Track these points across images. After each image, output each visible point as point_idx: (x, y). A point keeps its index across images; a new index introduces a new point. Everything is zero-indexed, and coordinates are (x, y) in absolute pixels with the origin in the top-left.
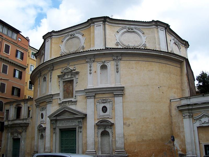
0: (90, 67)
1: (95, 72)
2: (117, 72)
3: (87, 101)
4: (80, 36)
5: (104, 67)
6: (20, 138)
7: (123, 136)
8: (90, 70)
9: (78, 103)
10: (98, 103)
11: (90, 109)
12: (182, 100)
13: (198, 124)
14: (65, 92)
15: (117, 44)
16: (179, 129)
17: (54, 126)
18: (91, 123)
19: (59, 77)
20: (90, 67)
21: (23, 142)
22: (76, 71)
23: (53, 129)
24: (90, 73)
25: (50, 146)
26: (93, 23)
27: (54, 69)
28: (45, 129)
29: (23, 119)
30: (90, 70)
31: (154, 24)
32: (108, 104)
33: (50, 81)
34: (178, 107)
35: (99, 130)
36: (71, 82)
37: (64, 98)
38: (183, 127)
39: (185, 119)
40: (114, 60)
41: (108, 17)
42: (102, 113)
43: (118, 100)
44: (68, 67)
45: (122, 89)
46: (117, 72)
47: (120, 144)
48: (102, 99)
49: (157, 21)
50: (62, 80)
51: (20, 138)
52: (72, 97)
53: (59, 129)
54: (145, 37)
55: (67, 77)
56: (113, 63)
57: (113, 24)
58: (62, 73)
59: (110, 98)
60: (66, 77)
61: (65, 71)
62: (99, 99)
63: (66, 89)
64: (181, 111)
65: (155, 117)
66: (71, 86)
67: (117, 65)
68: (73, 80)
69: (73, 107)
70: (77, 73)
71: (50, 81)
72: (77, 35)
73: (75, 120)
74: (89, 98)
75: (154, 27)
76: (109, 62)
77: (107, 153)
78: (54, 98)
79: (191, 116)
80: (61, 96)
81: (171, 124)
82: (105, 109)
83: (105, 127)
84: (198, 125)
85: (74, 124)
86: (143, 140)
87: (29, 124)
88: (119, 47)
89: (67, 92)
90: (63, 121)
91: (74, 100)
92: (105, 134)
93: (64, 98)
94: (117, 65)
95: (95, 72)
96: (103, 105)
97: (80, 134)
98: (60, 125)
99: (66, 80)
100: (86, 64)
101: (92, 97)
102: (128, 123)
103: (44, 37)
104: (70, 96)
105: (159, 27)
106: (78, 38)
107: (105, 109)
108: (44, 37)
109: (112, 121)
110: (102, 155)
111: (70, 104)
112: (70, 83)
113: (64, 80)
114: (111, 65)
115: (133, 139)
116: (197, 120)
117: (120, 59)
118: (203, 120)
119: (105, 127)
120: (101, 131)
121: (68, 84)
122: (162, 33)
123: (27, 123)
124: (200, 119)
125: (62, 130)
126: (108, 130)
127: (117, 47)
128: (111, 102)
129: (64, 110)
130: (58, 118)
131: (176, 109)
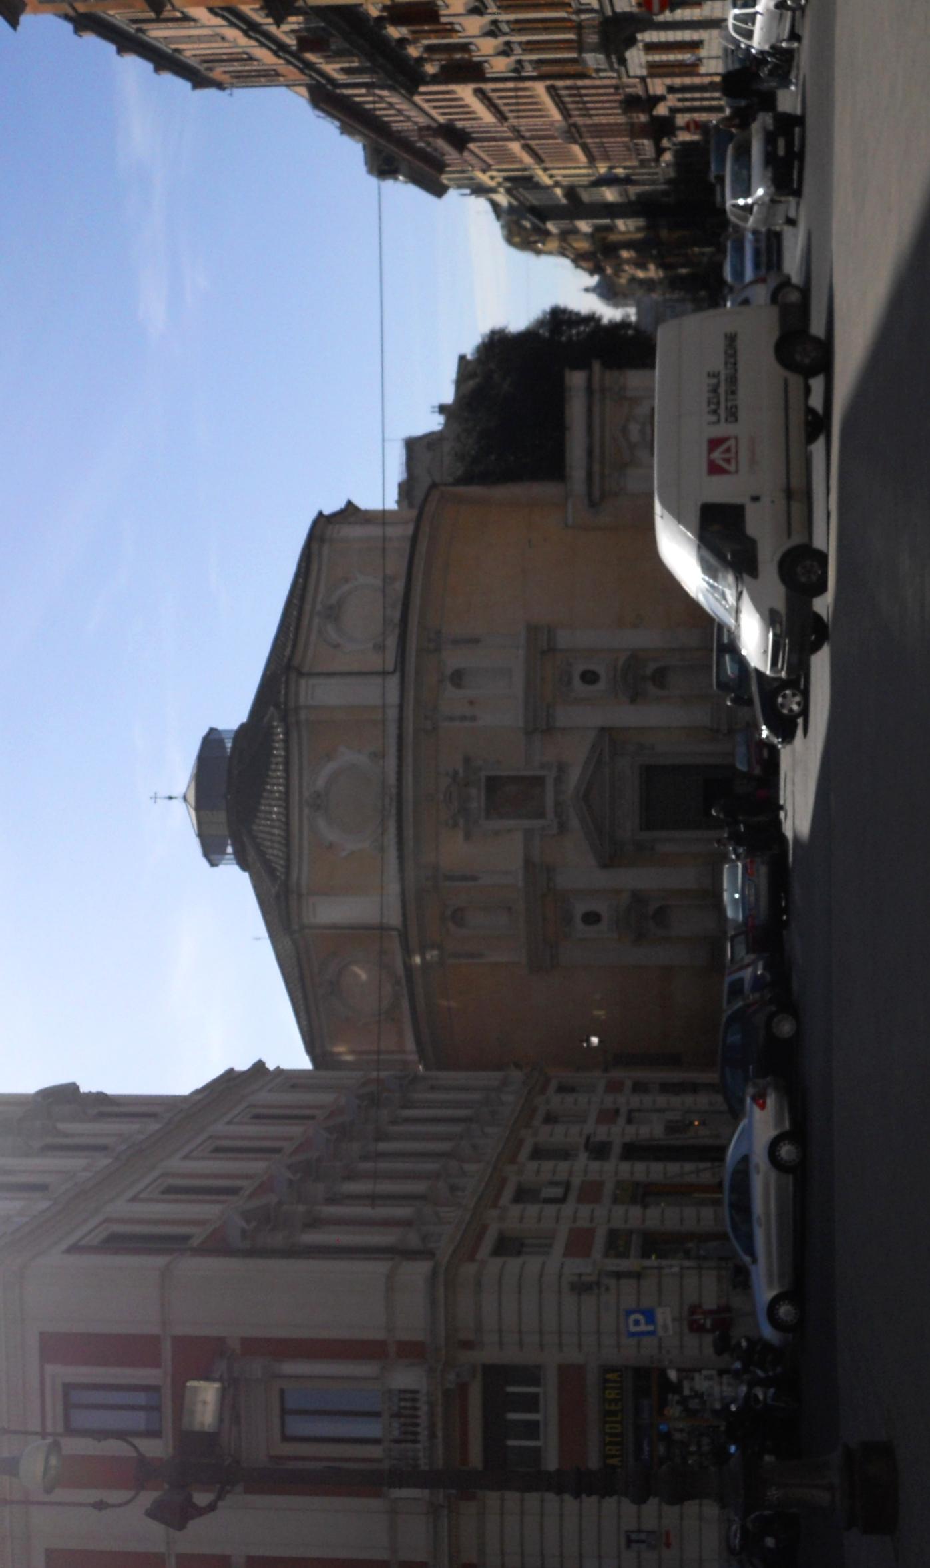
0: (451, 719)
1: (471, 703)
4: (329, 768)
5: (458, 678)
8: (463, 718)
11: (587, 716)
18: (627, 716)
20: (451, 719)
26: (297, 709)
28: (638, 899)
30: (463, 718)
33: (474, 878)
34: (592, 505)
36: (493, 784)
42: (602, 685)
43: (563, 639)
45: (533, 630)
53: (641, 829)
55: (477, 798)
58: (455, 825)
67: (456, 642)
69: (574, 776)
70: (467, 760)
71: (474, 878)
72: (320, 783)
75: (326, 550)
80: (537, 823)
82: (590, 677)
88: (392, 642)
93: (541, 815)
94: (456, 642)
95: (471, 703)
96: (577, 682)
107: (590, 677)
114: (454, 659)
117: (439, 632)
126: (651, 667)
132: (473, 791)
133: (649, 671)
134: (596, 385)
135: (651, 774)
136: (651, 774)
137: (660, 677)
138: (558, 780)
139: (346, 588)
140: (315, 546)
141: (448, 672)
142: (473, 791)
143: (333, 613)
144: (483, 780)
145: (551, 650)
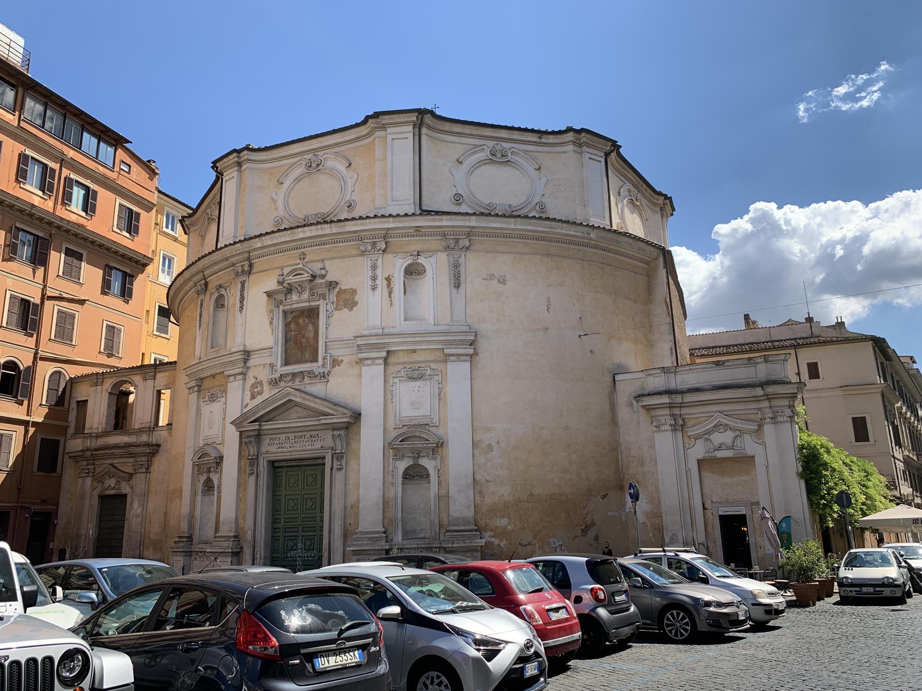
0: (374, 267)
2: (457, 286)
3: (363, 374)
6: (126, 495)
7: (471, 481)
8: (374, 278)
9: (330, 378)
10: (396, 380)
12: (650, 375)
13: (698, 451)
14: (291, 344)
15: (458, 199)
16: (642, 463)
17: (252, 454)
18: (371, 441)
19: (269, 294)
20: (374, 267)
21: (136, 505)
22: (329, 278)
23: (249, 463)
24: (374, 288)
25: (237, 518)
26: (383, 127)
27: (255, 270)
28: (219, 460)
29: (141, 431)
30: (374, 278)
31: (571, 139)
32: (428, 383)
33: (241, 308)
34: (639, 397)
35: (398, 463)
36: (312, 314)
37: (286, 363)
38: (654, 461)
39: (662, 434)
40: (447, 248)
41: (432, 113)
44: (301, 266)
46: (457, 286)
47: (461, 506)
48: (408, 367)
49: (583, 130)
50: (281, 307)
51: (126, 495)
52: (315, 359)
53: (269, 462)
54: (544, 180)
55: (298, 301)
56: (443, 257)
57: (443, 136)
58: (280, 283)
59: (433, 366)
60: (295, 297)
61: (291, 277)
62: (399, 367)
63: (293, 333)
64: (648, 409)
65: (567, 427)
66: (310, 327)
67: (456, 266)
68: (318, 308)
69: (317, 388)
72: (330, 163)
73: (320, 433)
74: (369, 362)
75: (571, 147)
76: (430, 254)
77: (422, 535)
78: (251, 363)
79: (680, 425)
81: (614, 447)
83: (415, 449)
84: (701, 456)
85: (318, 445)
86: (531, 494)
87: (159, 446)
89: (296, 344)
90: (283, 437)
91: (321, 370)
92: (415, 474)
94: (456, 266)
97: (339, 476)
98: (273, 449)
99: (294, 306)
100: (360, 259)
101: (377, 361)
102: (486, 442)
103: (218, 165)
104: (307, 356)
105: (585, 148)
106: (332, 173)
108: (218, 165)
109: (441, 432)
110: (405, 542)
111: (307, 380)
112: (307, 317)
113: (289, 307)
115: (501, 492)
116: (697, 438)
118: (718, 438)
119: (417, 454)
120: (402, 465)
121: (301, 321)
122: (593, 166)
123: (154, 442)
124: (706, 436)
125: (277, 464)
127: (455, 209)
128: (436, 378)
129: (286, 399)
130: (267, 426)
131: (631, 405)
132: (305, 296)
133: (424, 462)
134: (771, 389)
135: (311, 468)
136: (311, 468)
137: (415, 474)
138: (311, 374)
139: (531, 169)
140: (570, 136)
141: (421, 260)
142: (305, 296)
143: (499, 158)
144: (318, 303)
145: (446, 358)
